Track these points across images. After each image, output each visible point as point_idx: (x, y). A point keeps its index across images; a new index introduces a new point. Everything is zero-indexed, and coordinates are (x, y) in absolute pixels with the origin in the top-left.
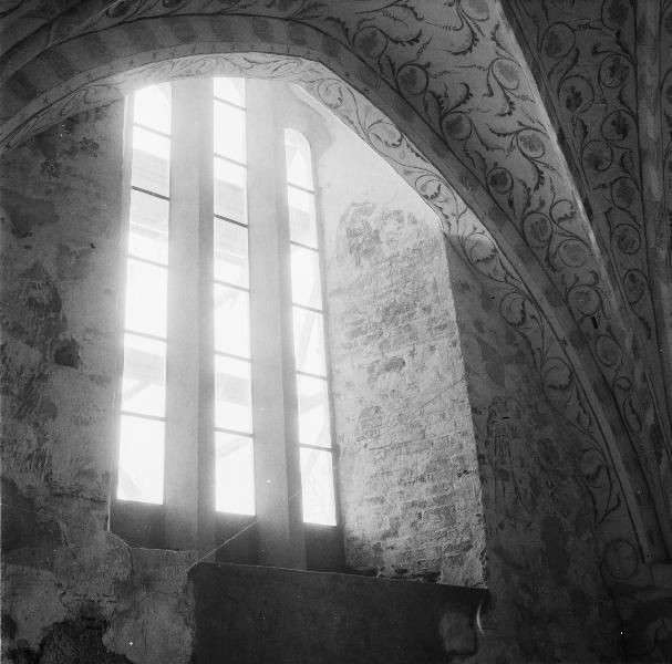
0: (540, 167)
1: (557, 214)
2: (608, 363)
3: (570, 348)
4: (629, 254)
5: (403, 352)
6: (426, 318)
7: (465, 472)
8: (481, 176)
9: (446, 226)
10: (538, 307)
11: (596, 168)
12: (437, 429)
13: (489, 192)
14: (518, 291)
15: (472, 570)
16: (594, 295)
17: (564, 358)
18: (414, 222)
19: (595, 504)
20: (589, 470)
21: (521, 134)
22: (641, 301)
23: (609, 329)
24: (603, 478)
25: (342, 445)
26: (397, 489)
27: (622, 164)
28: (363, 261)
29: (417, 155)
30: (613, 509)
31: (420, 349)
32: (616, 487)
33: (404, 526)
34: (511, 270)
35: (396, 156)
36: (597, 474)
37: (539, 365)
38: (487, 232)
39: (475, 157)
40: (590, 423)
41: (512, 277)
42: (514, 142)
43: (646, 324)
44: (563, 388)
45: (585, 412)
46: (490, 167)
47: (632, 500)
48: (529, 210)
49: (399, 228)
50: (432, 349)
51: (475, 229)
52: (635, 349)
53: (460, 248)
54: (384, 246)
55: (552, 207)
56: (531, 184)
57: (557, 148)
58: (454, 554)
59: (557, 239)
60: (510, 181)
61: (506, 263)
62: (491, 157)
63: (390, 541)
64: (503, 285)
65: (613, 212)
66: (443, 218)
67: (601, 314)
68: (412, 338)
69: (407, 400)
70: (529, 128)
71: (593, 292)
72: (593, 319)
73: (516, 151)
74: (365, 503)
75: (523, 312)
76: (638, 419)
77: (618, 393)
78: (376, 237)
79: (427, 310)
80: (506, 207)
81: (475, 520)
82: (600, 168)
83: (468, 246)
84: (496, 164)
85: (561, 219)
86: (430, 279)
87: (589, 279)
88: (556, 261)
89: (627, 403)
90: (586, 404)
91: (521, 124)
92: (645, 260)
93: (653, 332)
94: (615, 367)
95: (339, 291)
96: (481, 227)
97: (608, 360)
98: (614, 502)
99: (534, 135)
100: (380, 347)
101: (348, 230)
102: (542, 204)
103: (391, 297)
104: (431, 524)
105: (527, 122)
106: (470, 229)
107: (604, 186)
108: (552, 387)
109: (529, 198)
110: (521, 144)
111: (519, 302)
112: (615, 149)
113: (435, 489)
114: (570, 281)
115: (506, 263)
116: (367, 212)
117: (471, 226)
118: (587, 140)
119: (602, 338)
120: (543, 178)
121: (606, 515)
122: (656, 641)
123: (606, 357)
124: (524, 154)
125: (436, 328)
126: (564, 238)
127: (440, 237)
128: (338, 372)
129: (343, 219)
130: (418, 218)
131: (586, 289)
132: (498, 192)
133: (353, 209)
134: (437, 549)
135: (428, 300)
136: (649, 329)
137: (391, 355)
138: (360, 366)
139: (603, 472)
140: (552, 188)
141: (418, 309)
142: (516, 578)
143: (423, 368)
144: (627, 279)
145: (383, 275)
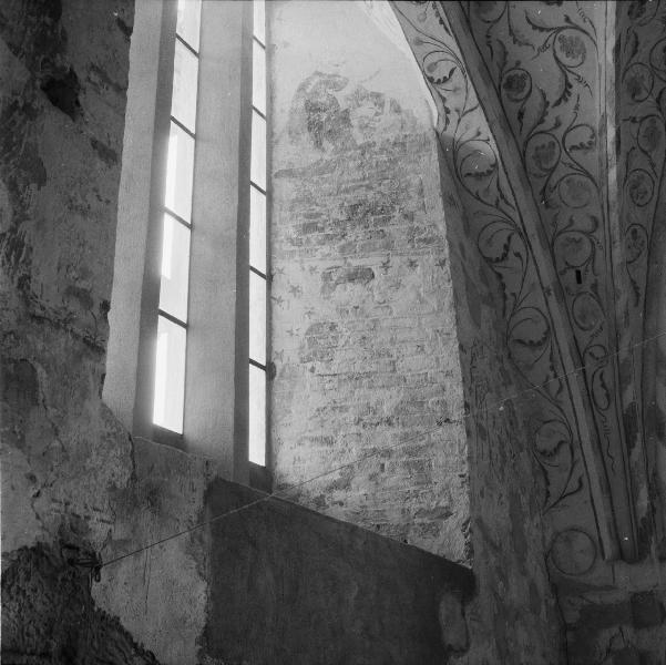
0: (571, 78)
1: (572, 140)
2: (582, 325)
3: (552, 299)
4: (638, 205)
5: (373, 261)
6: (406, 225)
7: (447, 420)
8: (496, 76)
9: (442, 125)
11: (633, 96)
12: (413, 363)
13: (499, 95)
14: (510, 220)
15: (452, 542)
16: (587, 247)
17: (544, 310)
18: (398, 110)
19: (548, 483)
20: (545, 443)
21: (564, 32)
23: (595, 286)
24: (564, 456)
25: (279, 364)
26: (354, 429)
27: (658, 101)
28: (326, 143)
29: (441, 22)
31: (396, 261)
32: (579, 470)
33: (360, 478)
34: (508, 194)
35: (413, 18)
36: (556, 450)
37: (508, 314)
38: (492, 142)
39: (496, 48)
40: (559, 391)
41: (507, 203)
42: (550, 41)
43: (636, 289)
45: (556, 376)
46: (511, 64)
48: (540, 128)
49: (377, 114)
50: (412, 264)
51: (479, 134)
53: (451, 155)
54: (355, 132)
55: (568, 131)
56: (553, 97)
57: (610, 57)
58: (427, 520)
59: (562, 171)
60: (527, 89)
61: (504, 184)
62: (516, 53)
63: (339, 495)
64: (493, 211)
65: (634, 152)
66: (443, 112)
68: (388, 246)
69: (373, 321)
70: (576, 27)
71: (586, 240)
72: (578, 273)
73: (549, 53)
74: (307, 443)
75: (506, 247)
76: (608, 396)
78: (345, 118)
79: (409, 217)
80: (513, 117)
81: (458, 481)
82: (637, 97)
83: (462, 153)
84: (518, 63)
85: (573, 147)
86: (416, 181)
87: (587, 225)
88: (553, 196)
89: (598, 374)
90: (559, 367)
91: (567, 19)
92: (652, 216)
93: (642, 298)
95: (290, 173)
96: (486, 133)
97: (584, 322)
98: (574, 484)
99: (577, 39)
100: (342, 250)
101: (306, 104)
102: (558, 124)
103: (361, 193)
104: (396, 479)
105: (576, 19)
106: (471, 133)
107: (634, 120)
108: (520, 341)
109: (545, 113)
110: (558, 44)
112: (656, 79)
113: (405, 437)
114: (563, 222)
115: (504, 184)
116: (337, 87)
117: (477, 132)
118: (635, 60)
120: (570, 94)
121: (561, 498)
122: (609, 651)
123: (583, 318)
124: (556, 59)
125: (420, 240)
126: (571, 171)
127: (431, 136)
128: (281, 272)
129: (302, 88)
130: (404, 107)
131: (577, 236)
132: (508, 96)
133: (317, 79)
134: (403, 511)
135: (411, 205)
136: (638, 295)
137: (355, 263)
138: (313, 270)
139: (565, 449)
140: (577, 108)
141: (397, 214)
142: (493, 559)
143: (398, 285)
144: (629, 235)
145: (351, 164)
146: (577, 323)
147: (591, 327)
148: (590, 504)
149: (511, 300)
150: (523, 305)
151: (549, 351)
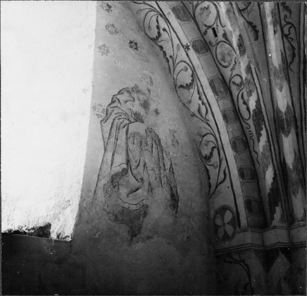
3: (192, 52)
10: (167, 20)
17: (187, 60)
20: (206, 151)
22: (249, 8)
23: (225, 35)
24: (215, 159)
30: (221, 183)
36: (211, 154)
37: (172, 71)
44: (188, 87)
45: (203, 103)
47: (235, 172)
52: (241, 45)
67: (219, 24)
72: (214, 29)
75: (158, 27)
77: (234, 88)
89: (241, 93)
90: (203, 97)
93: (260, 34)
94: (231, 67)
97: (225, 62)
98: (222, 176)
108: (182, 86)
111: (155, 17)
119: (219, 46)
121: (217, 186)
136: (256, 32)
139: (215, 152)
146: (221, 64)
147: (230, 64)
148: (230, 189)
149: (171, 60)
150: (177, 62)
151: (196, 87)
